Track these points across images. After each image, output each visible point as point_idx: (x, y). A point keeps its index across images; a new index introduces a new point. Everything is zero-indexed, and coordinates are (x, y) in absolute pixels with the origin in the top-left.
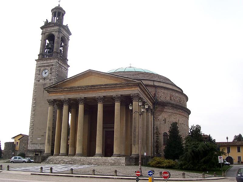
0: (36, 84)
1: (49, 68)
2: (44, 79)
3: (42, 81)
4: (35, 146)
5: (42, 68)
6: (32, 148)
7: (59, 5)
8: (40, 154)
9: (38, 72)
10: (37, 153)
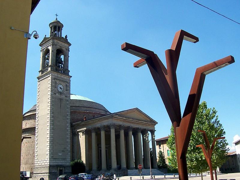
2: (61, 93)
5: (58, 82)
7: (57, 19)
9: (54, 84)
10: (61, 169)
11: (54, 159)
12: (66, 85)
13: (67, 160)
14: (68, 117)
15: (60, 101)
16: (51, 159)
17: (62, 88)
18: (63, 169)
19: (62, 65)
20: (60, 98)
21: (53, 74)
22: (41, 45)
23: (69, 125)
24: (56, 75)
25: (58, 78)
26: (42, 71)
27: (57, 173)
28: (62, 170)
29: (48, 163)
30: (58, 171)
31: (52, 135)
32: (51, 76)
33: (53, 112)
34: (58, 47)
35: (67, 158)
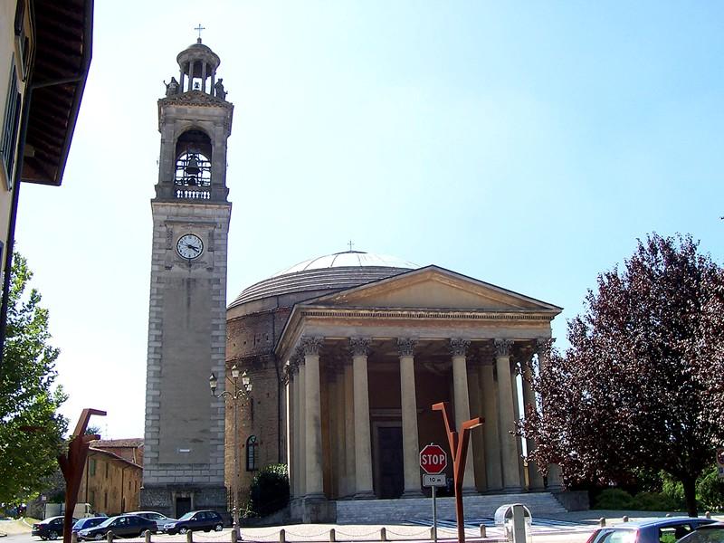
0: (156, 279)
1: (205, 232)
2: (190, 263)
4: (173, 473)
5: (178, 230)
6: (162, 480)
7: (199, 40)
9: (164, 241)
10: (184, 496)
11: (161, 465)
12: (211, 235)
15: (189, 287)
17: (196, 243)
18: (192, 496)
25: (180, 219)
27: (169, 508)
31: (157, 393)
34: (184, 125)
35: (211, 461)
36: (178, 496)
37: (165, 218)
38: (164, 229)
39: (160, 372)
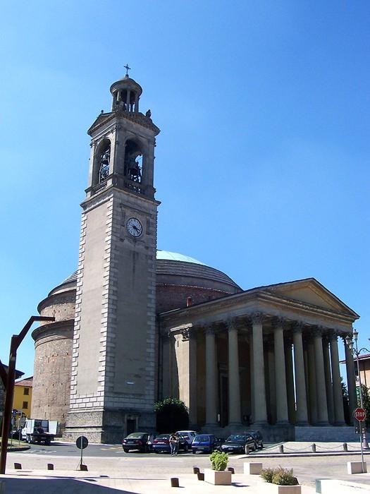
2: (135, 239)
3: (130, 244)
4: (123, 400)
5: (128, 213)
6: (116, 405)
7: (127, 75)
8: (139, 419)
10: (132, 418)
11: (116, 393)
12: (148, 222)
13: (147, 398)
14: (150, 296)
15: (134, 257)
16: (108, 394)
17: (139, 227)
18: (137, 418)
19: (139, 178)
20: (133, 250)
21: (118, 194)
22: (91, 132)
23: (152, 315)
24: (126, 197)
26: (92, 190)
27: (121, 427)
28: (134, 421)
29: (102, 404)
30: (124, 423)
31: (114, 336)
32: (112, 199)
33: (115, 281)
34: (130, 136)
35: (146, 393)
36: (129, 418)
37: (120, 202)
38: (120, 210)
39: (116, 320)
